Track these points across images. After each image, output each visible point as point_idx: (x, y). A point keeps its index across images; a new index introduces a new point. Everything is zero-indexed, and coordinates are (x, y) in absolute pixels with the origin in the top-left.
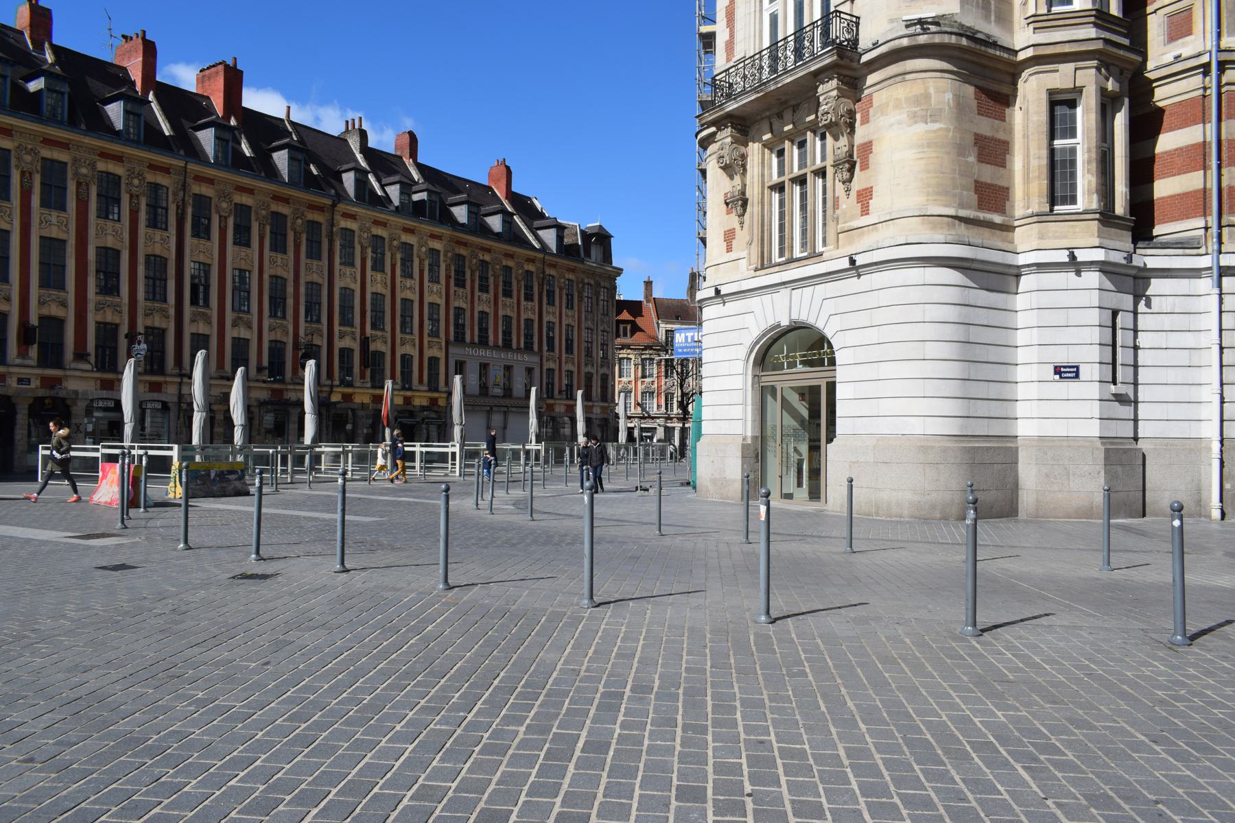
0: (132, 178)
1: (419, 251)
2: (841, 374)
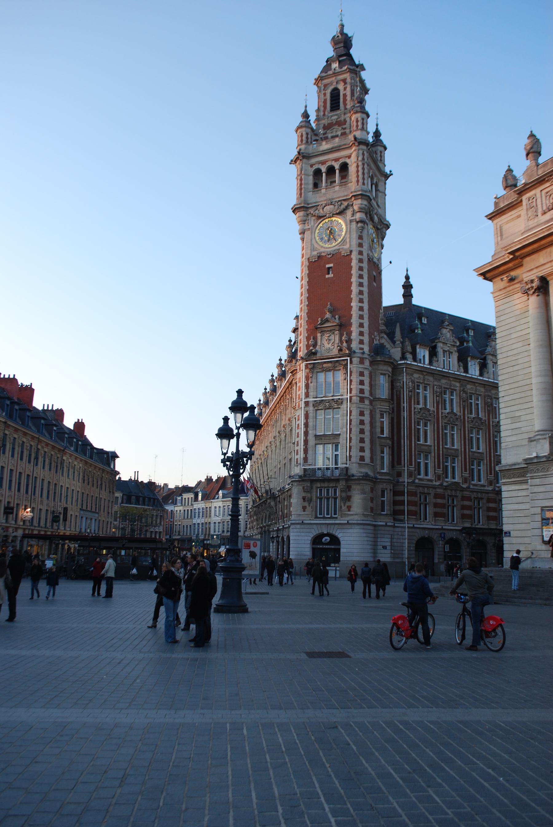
2: (342, 546)
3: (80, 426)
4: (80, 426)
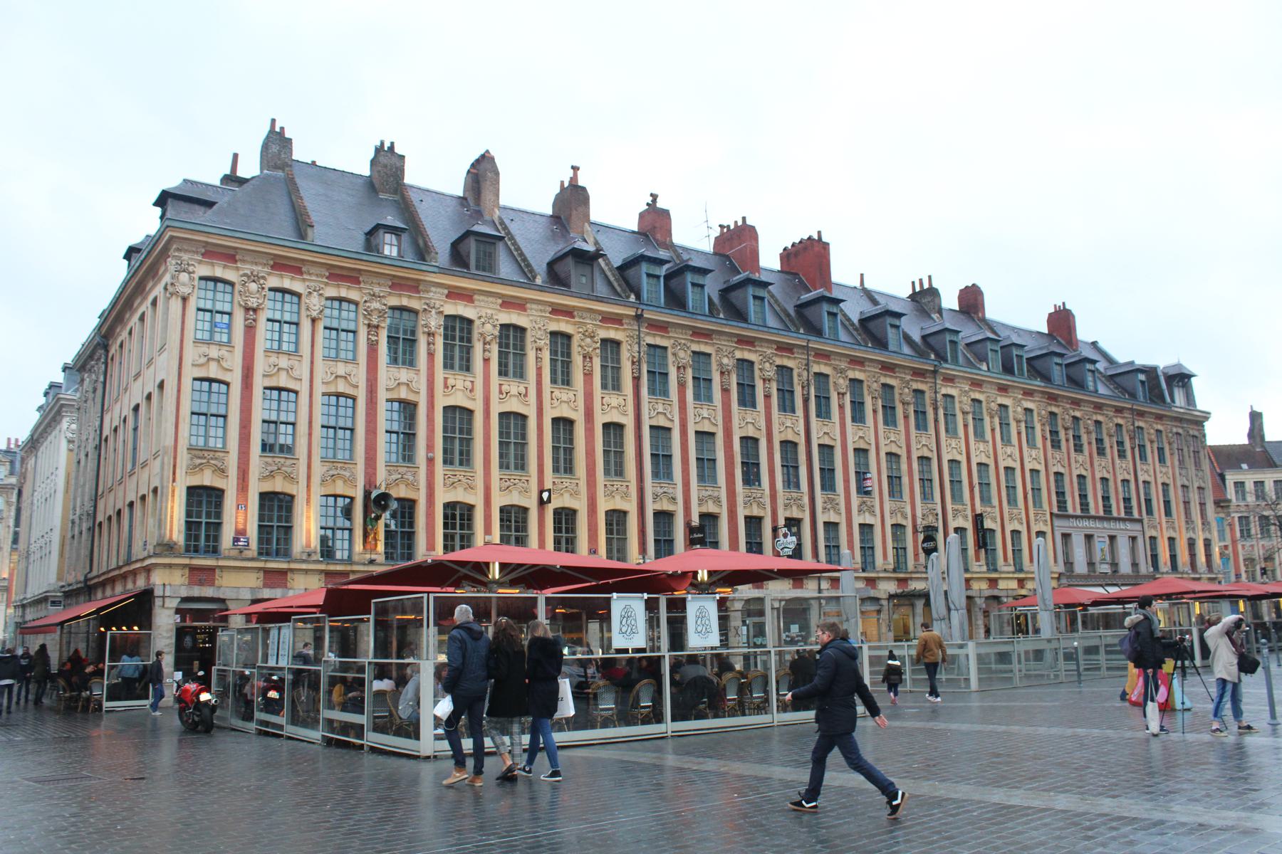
0: (768, 361)
1: (1016, 411)
3: (1062, 321)
4: (1062, 321)
